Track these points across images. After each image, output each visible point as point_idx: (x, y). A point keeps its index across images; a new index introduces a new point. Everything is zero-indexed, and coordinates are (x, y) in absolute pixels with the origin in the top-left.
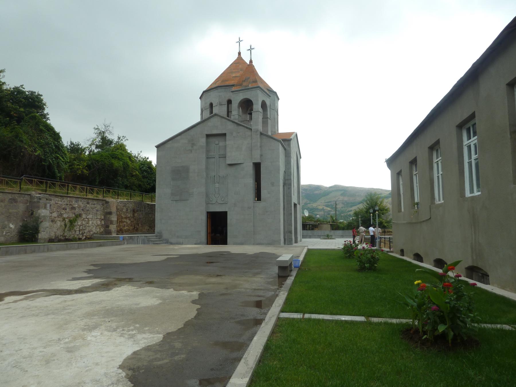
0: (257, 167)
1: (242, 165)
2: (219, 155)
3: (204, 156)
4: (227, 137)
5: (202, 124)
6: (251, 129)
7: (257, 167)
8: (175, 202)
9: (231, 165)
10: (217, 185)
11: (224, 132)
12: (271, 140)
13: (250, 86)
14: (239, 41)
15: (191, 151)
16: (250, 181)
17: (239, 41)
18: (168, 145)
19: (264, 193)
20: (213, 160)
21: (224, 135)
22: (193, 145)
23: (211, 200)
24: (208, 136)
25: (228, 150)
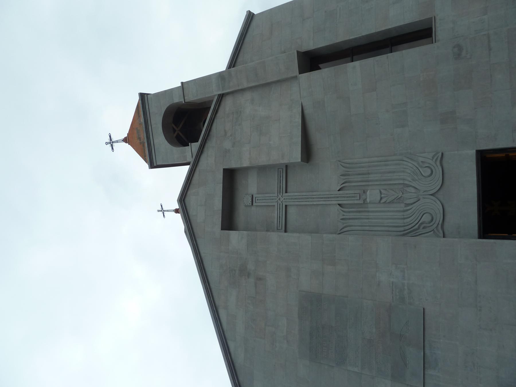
0: (312, 61)
1: (306, 112)
2: (279, 192)
3: (274, 236)
4: (233, 165)
5: (199, 241)
6: (221, 97)
7: (312, 61)
8: (429, 372)
9: (307, 152)
10: (373, 195)
11: (220, 176)
12: (247, 40)
13: (142, 120)
14: (163, 211)
15: (259, 279)
16: (355, 70)
17: (163, 211)
18: (239, 359)
19: (400, 16)
20: (292, 211)
21: (230, 176)
22: (244, 271)
23: (426, 218)
24: (229, 222)
25: (263, 160)
